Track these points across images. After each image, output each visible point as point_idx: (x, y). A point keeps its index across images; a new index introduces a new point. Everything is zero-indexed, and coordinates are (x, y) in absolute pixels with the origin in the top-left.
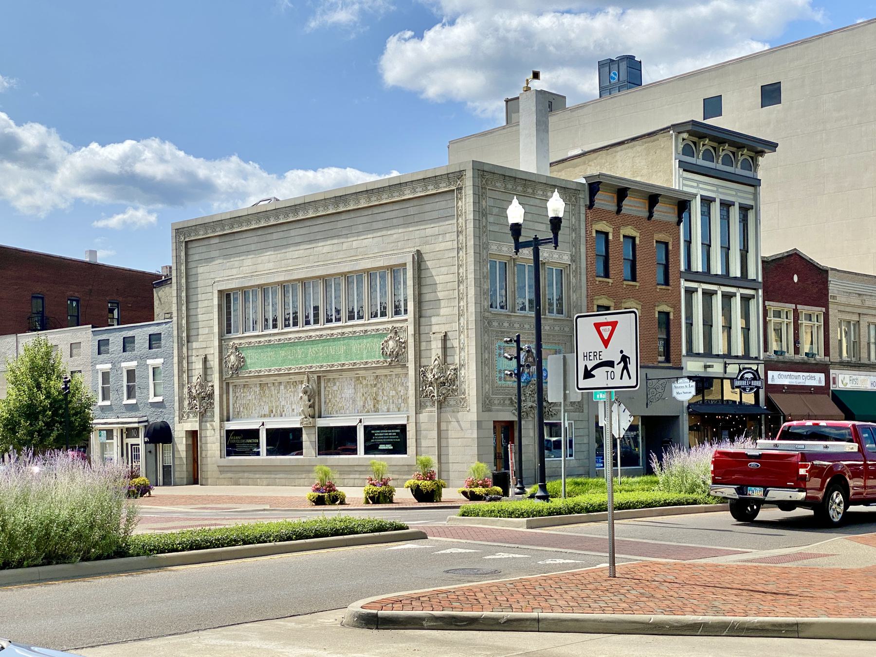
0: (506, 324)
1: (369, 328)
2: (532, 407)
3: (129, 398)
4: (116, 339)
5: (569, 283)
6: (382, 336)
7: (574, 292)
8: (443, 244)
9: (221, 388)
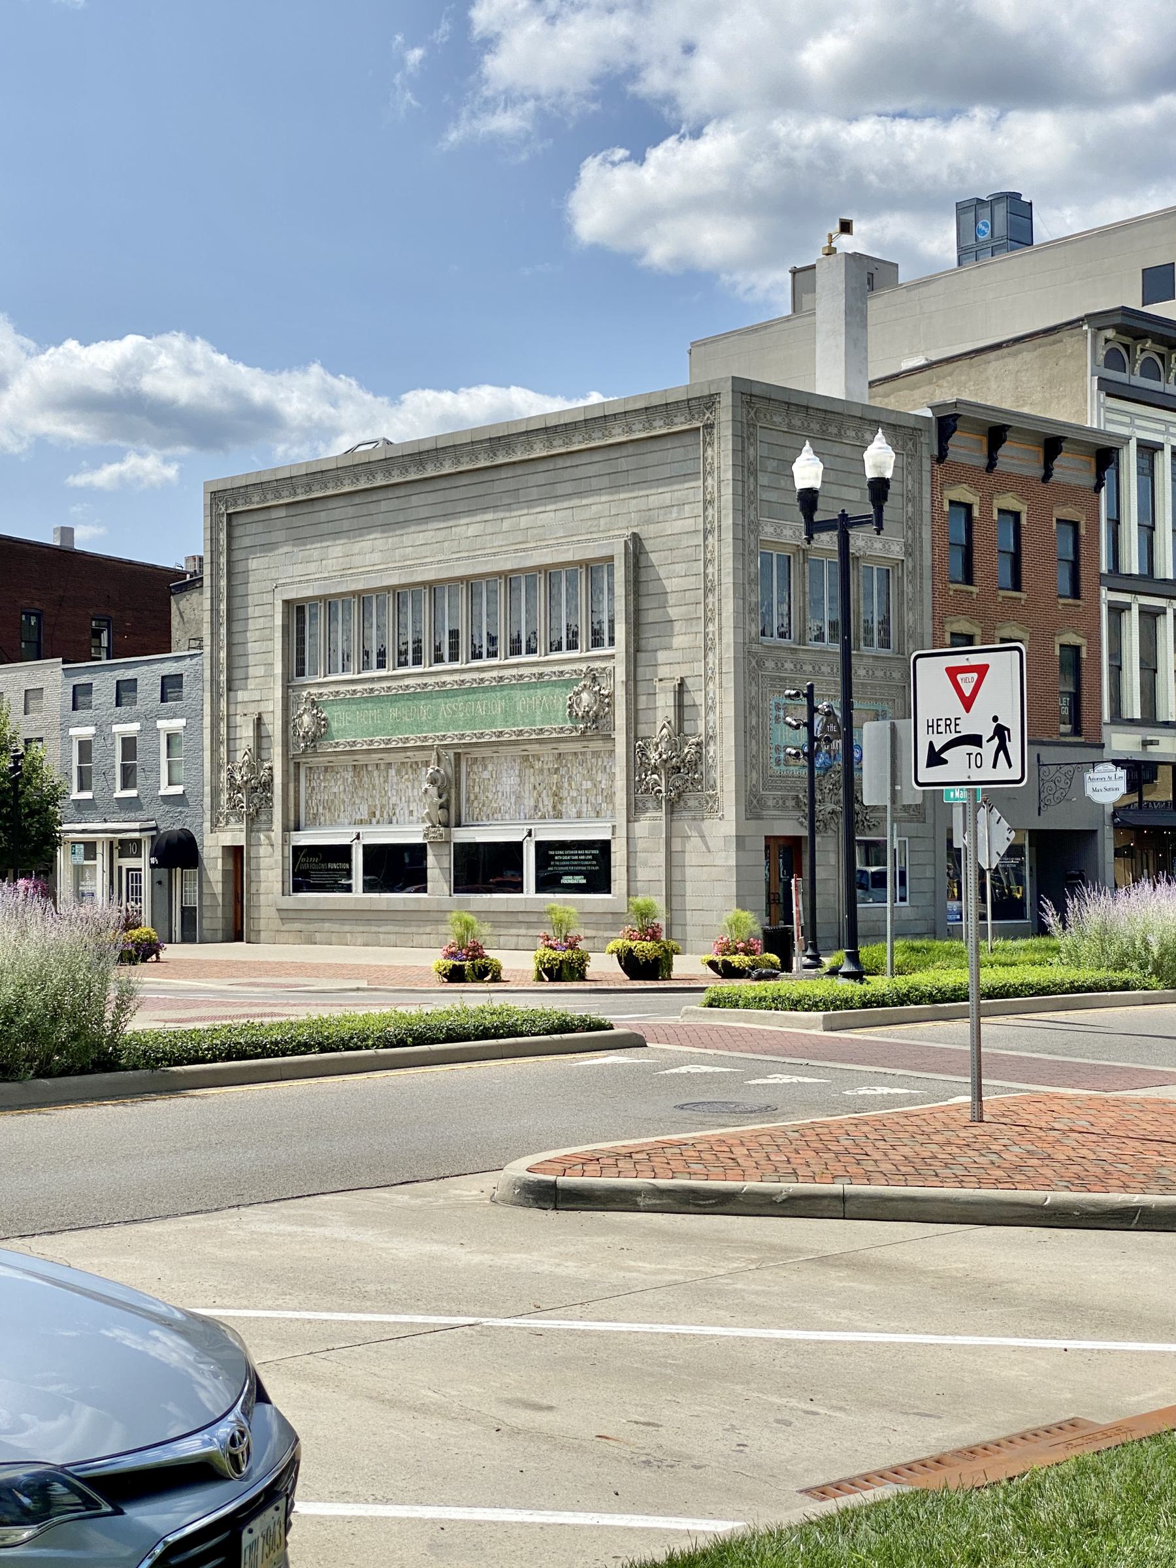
0: (789, 665)
1: (547, 670)
2: (833, 812)
3: (125, 786)
4: (104, 683)
5: (901, 593)
6: (568, 684)
7: (910, 609)
8: (680, 523)
9: (285, 772)
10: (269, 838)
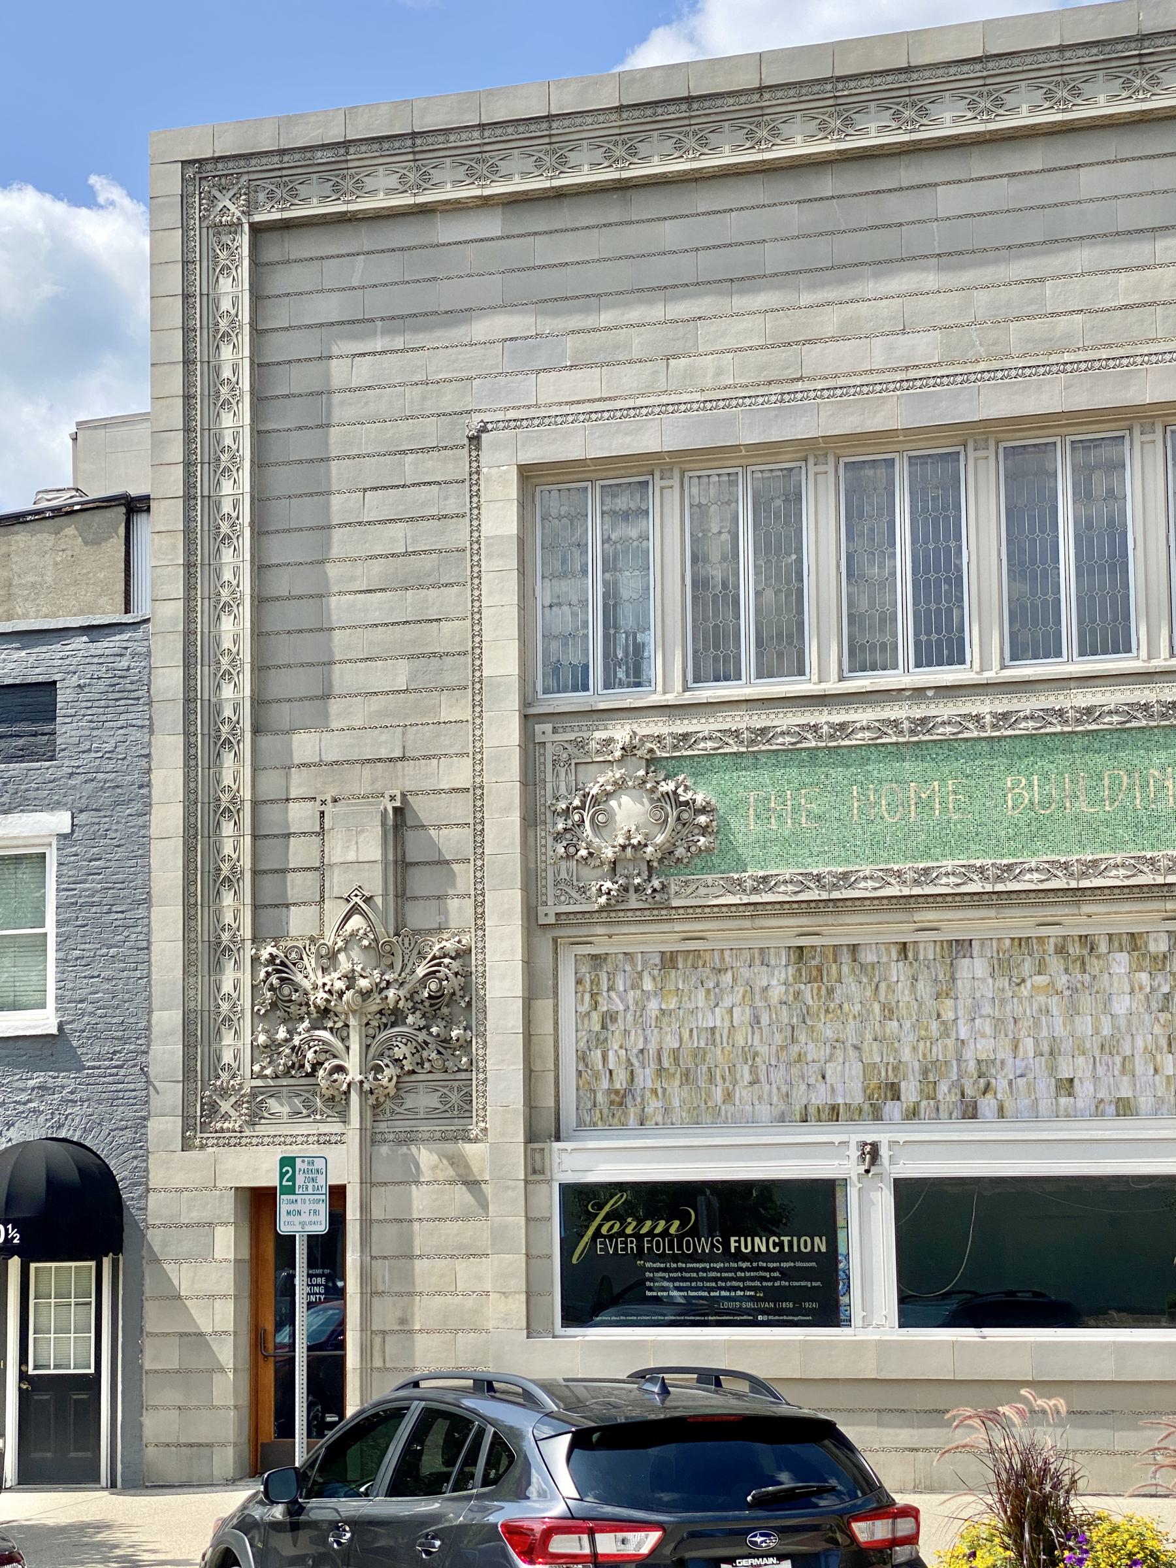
10: (457, 1161)
